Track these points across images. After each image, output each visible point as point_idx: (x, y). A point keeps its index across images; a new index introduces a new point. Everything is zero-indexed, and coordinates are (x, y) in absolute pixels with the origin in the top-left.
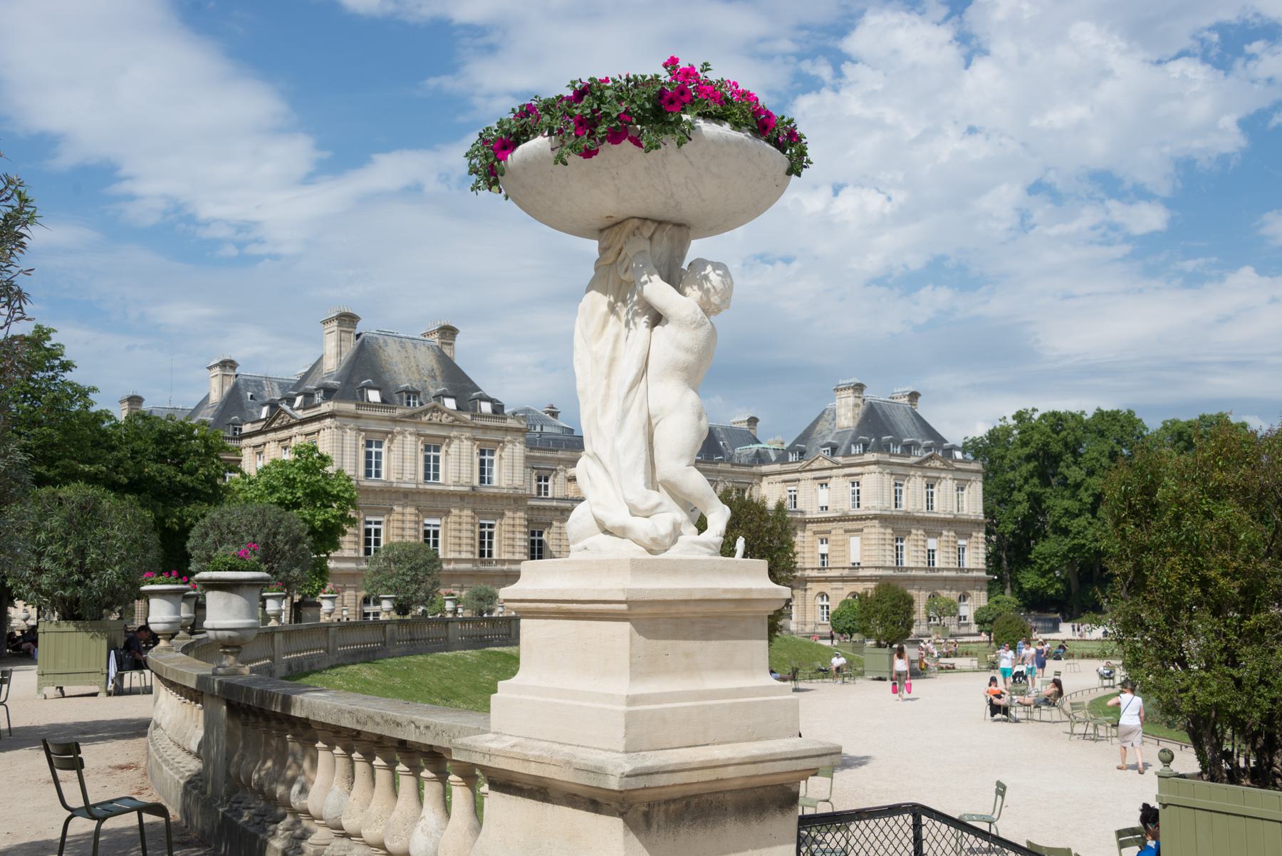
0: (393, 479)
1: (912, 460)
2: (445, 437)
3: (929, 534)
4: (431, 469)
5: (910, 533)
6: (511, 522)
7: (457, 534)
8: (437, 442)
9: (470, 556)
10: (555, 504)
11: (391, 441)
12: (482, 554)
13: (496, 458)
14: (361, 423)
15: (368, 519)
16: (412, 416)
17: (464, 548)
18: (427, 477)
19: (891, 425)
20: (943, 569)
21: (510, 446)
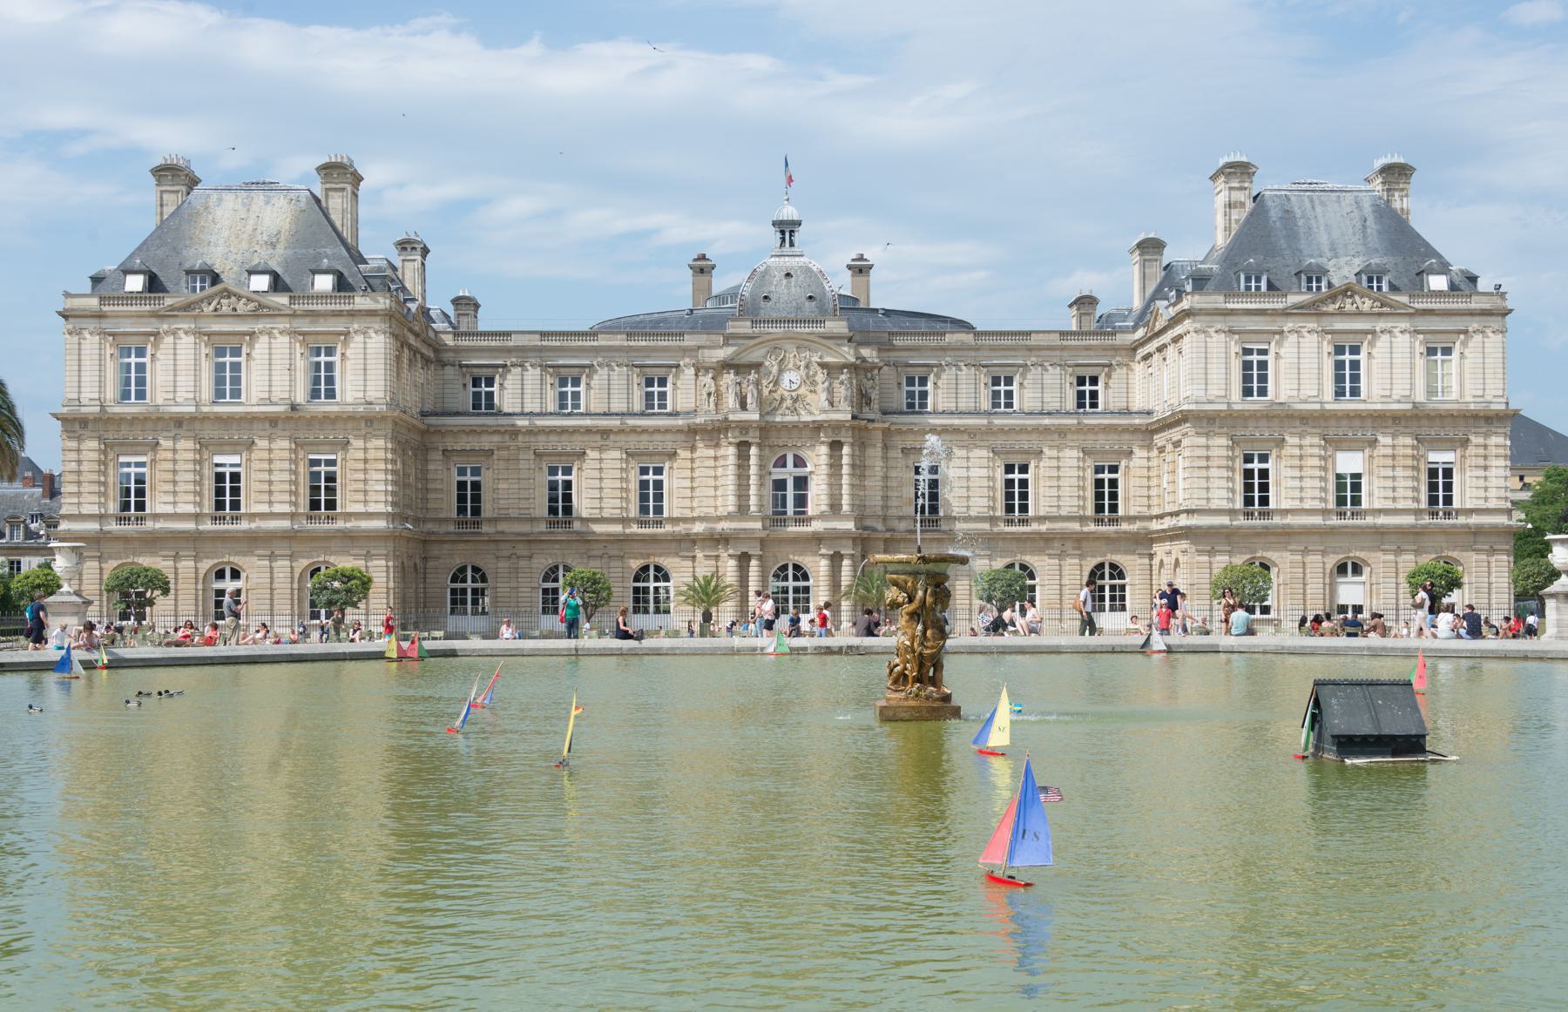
0: (160, 401)
1: (1293, 299)
2: (244, 334)
3: (1336, 443)
4: (227, 382)
5: (1281, 443)
6: (361, 455)
7: (266, 476)
8: (234, 342)
9: (286, 508)
10: (588, 422)
11: (156, 346)
12: (315, 505)
13: (336, 359)
14: (108, 325)
15: (122, 459)
16: (188, 307)
17: (276, 497)
18: (220, 394)
19: (1292, 235)
20: (1380, 511)
21: (359, 338)
